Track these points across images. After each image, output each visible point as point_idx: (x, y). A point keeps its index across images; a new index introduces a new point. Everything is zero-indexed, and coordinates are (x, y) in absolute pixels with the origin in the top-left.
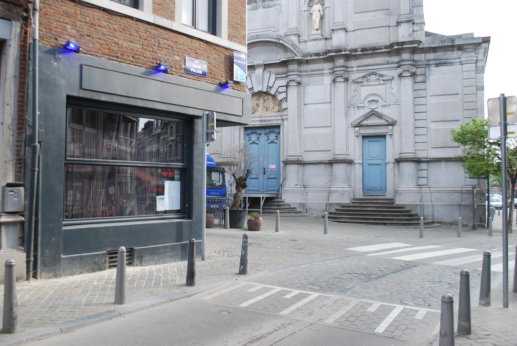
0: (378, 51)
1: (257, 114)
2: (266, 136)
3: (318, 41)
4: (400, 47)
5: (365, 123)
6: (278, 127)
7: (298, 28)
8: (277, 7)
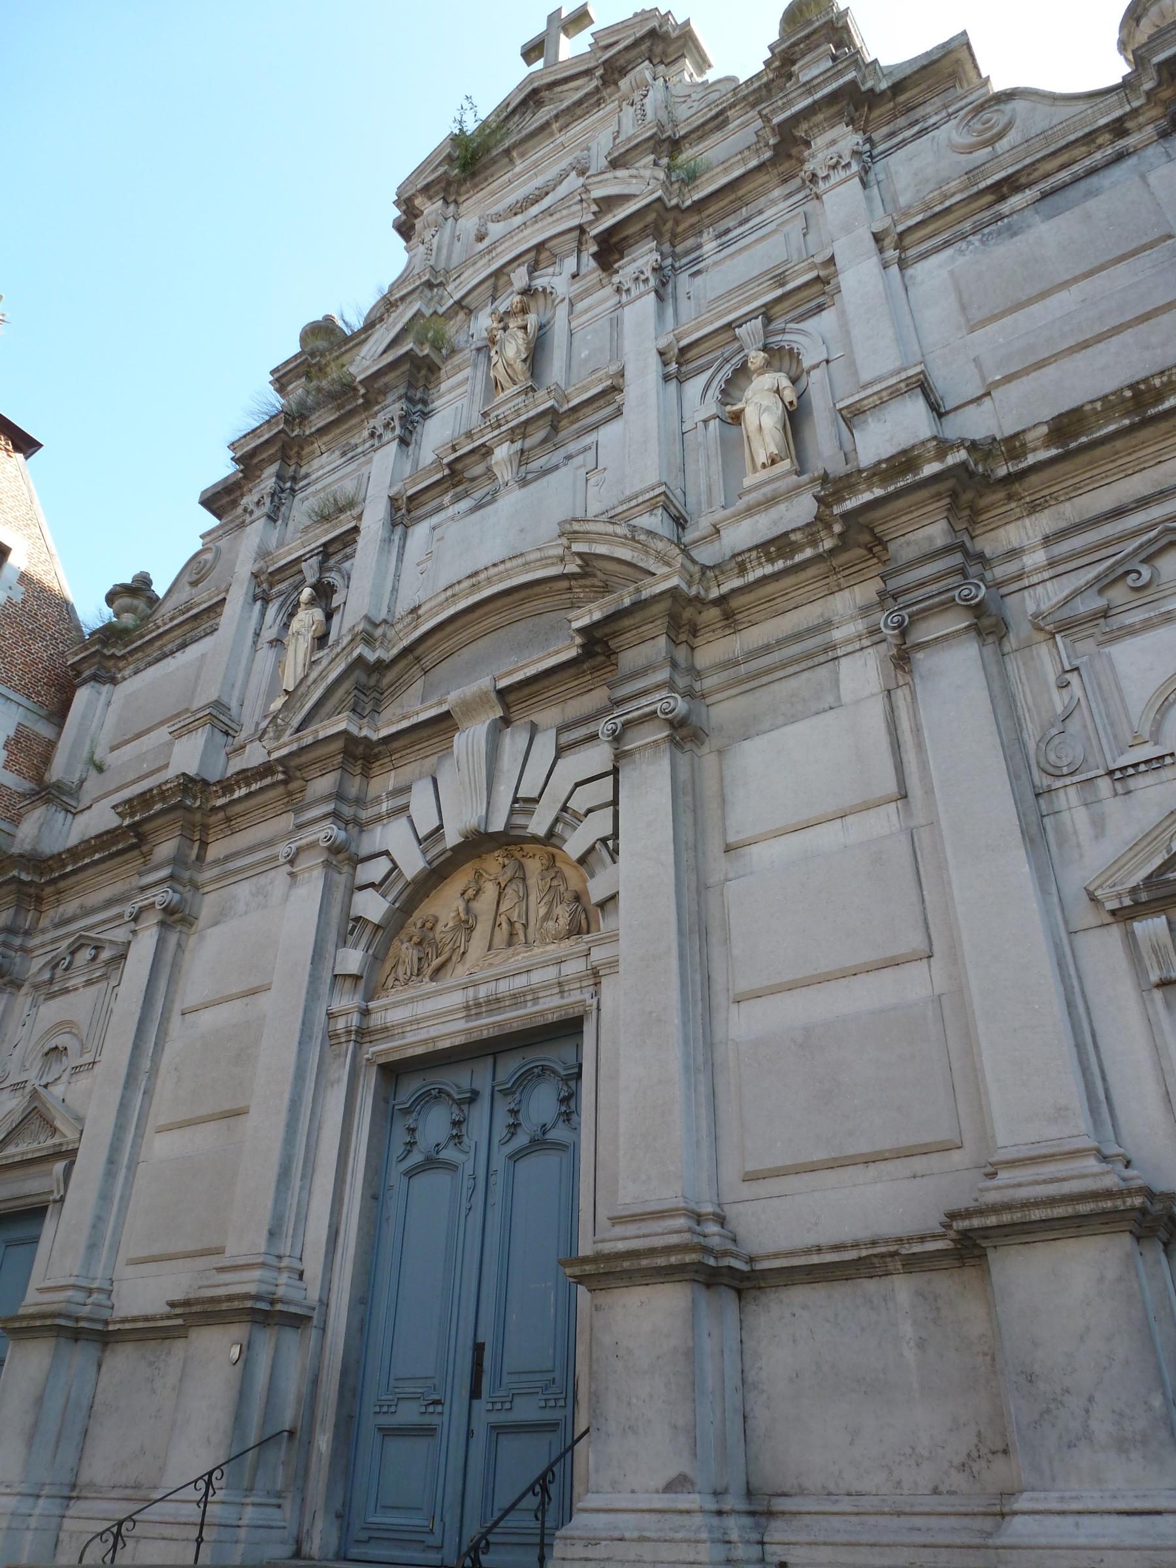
1: (459, 973)
2: (502, 1106)
3: (782, 507)
6: (569, 1028)
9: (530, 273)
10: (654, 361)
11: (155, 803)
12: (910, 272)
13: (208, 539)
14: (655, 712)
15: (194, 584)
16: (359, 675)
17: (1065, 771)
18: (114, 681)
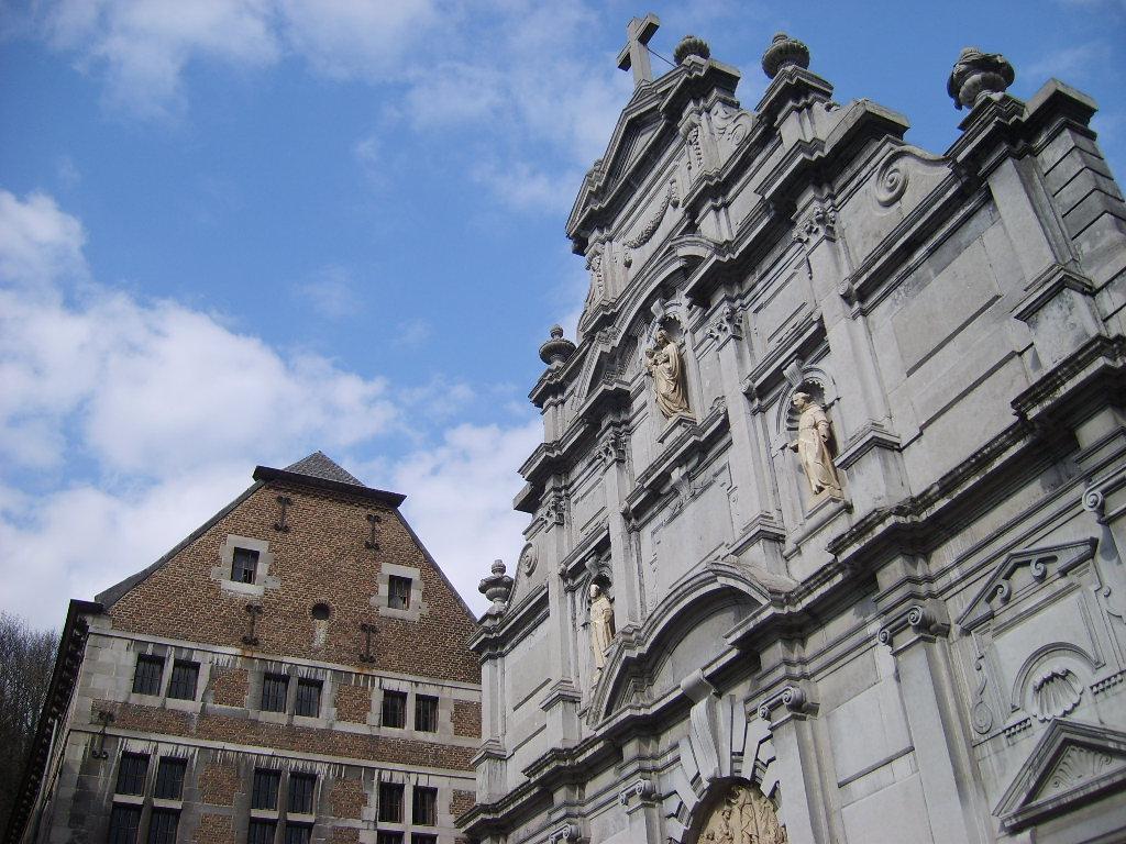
0: (998, 463)
4: (1047, 403)
5: (1051, 793)
7: (774, 514)
8: (720, 479)
9: (662, 304)
10: (743, 400)
11: (543, 767)
12: (870, 317)
13: (528, 534)
14: (781, 700)
15: (529, 574)
16: (634, 669)
17: (984, 730)
18: (502, 655)
